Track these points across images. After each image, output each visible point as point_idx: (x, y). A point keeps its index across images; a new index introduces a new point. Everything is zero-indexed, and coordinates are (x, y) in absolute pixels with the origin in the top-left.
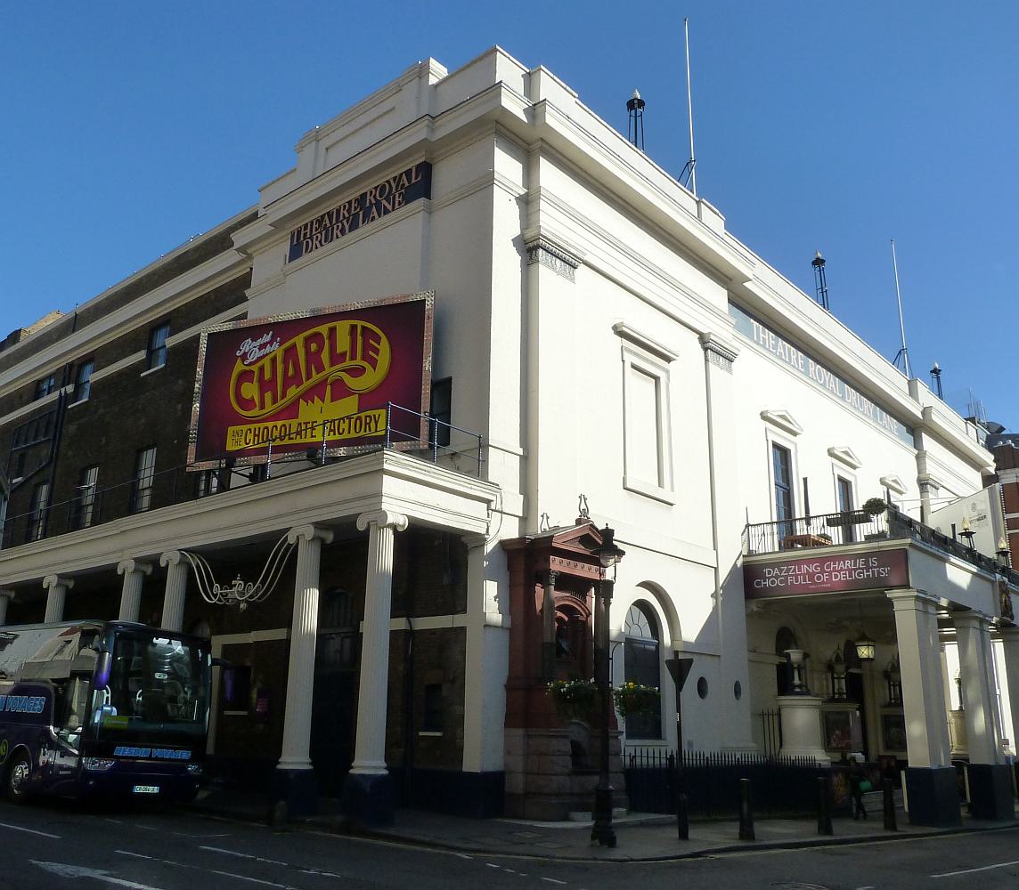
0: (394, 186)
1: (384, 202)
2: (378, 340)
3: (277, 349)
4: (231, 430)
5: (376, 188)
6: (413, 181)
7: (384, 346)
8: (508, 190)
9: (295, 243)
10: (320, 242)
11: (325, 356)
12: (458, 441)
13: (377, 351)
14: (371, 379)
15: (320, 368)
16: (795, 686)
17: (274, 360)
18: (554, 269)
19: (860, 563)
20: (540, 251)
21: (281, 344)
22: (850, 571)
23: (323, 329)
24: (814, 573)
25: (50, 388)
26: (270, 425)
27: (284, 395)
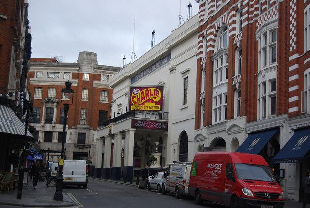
3: (140, 92)
7: (160, 93)
11: (149, 95)
14: (158, 99)
15: (148, 97)
23: (149, 89)
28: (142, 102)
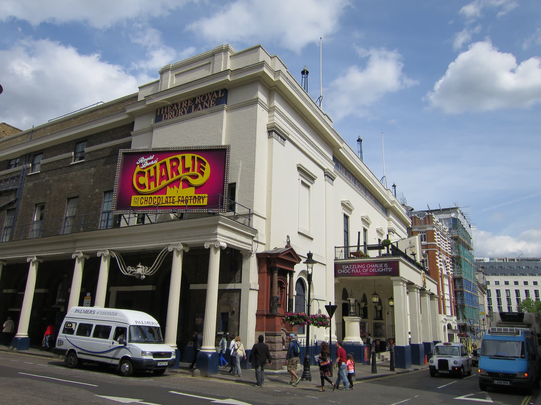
0: (210, 97)
1: (205, 103)
2: (205, 164)
3: (156, 163)
4: (133, 197)
5: (201, 96)
6: (220, 96)
7: (208, 167)
8: (262, 106)
9: (158, 114)
10: (172, 116)
11: (180, 168)
12: (238, 210)
13: (204, 169)
14: (201, 181)
15: (178, 173)
16: (351, 313)
17: (155, 168)
18: (278, 140)
19: (381, 265)
20: (274, 133)
21: (158, 161)
22: (377, 268)
23: (179, 157)
24: (363, 268)
25: (16, 164)
26: (153, 196)
27: (160, 184)
28: (158, 187)
